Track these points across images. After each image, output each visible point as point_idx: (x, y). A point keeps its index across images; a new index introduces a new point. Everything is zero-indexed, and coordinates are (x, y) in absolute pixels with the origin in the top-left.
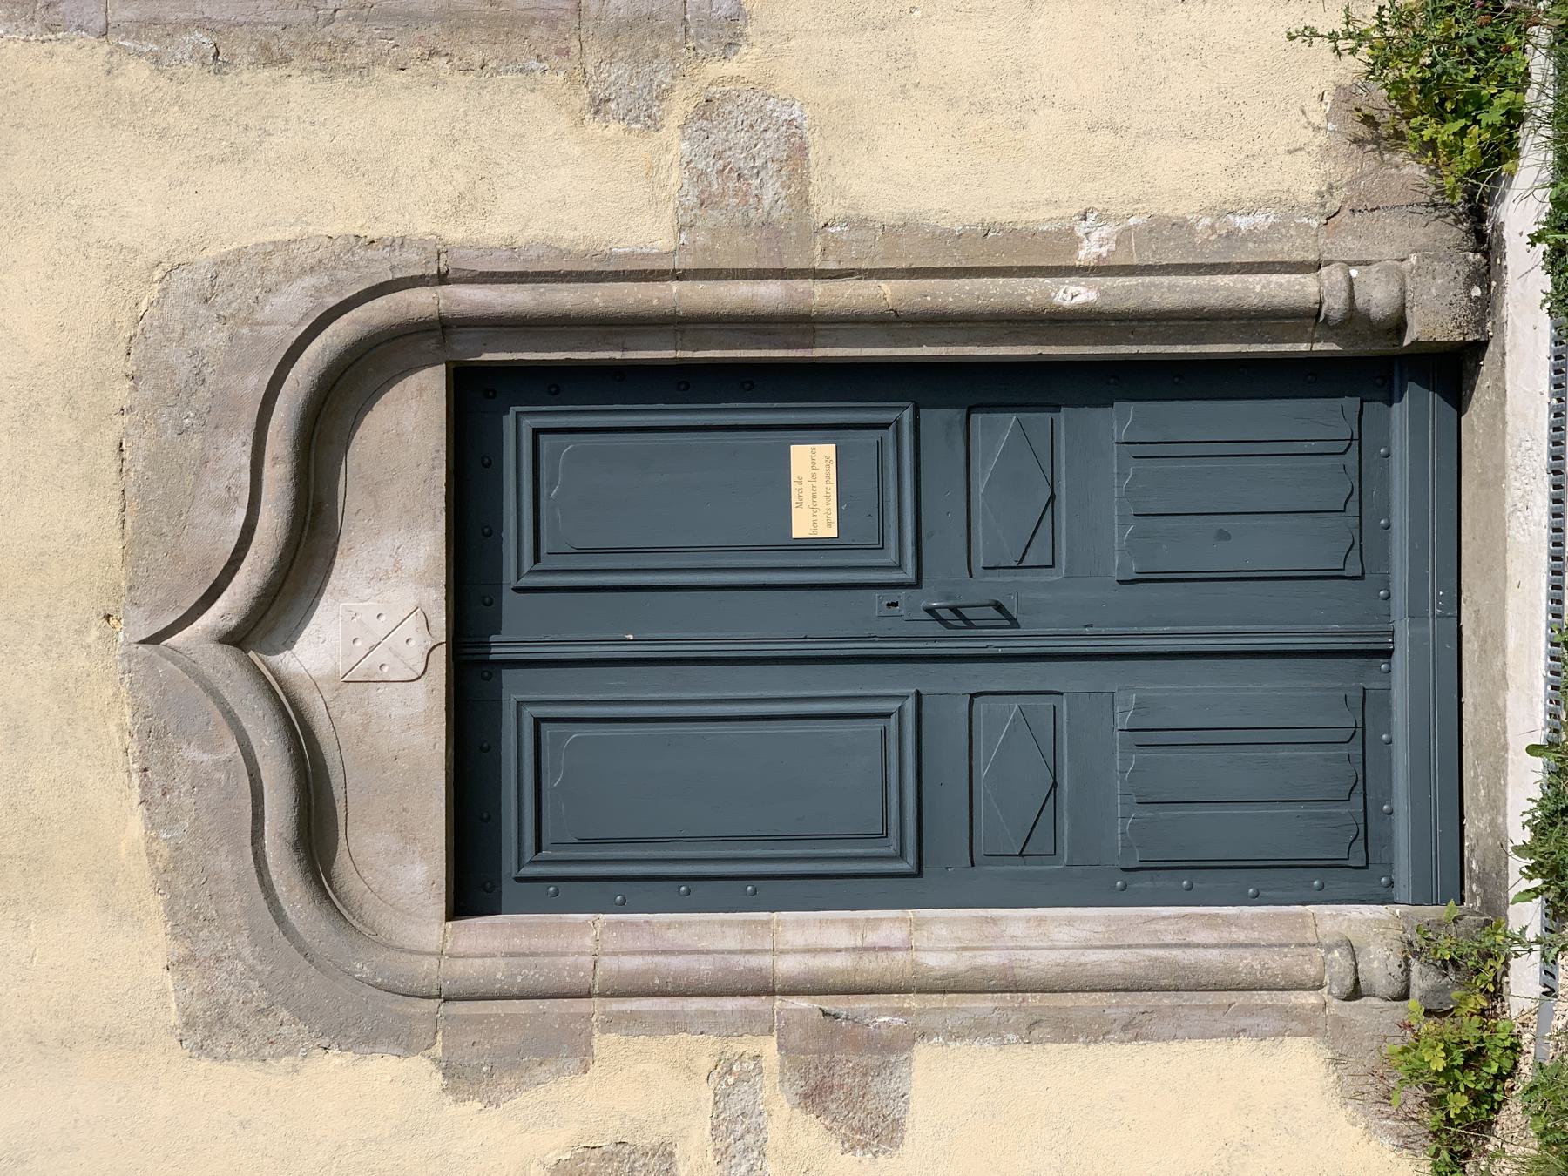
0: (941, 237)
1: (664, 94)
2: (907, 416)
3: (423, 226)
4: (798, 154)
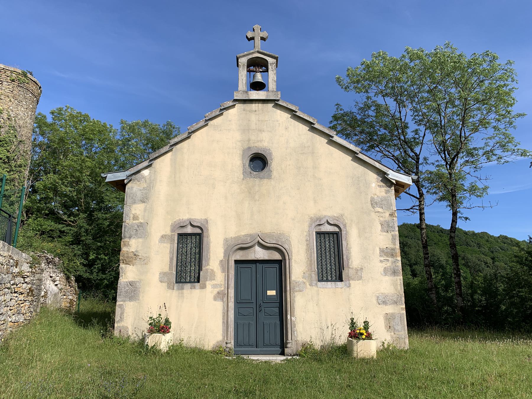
0: (294, 304)
1: (305, 279)
2: (278, 301)
3: (293, 258)
4: (300, 291)
